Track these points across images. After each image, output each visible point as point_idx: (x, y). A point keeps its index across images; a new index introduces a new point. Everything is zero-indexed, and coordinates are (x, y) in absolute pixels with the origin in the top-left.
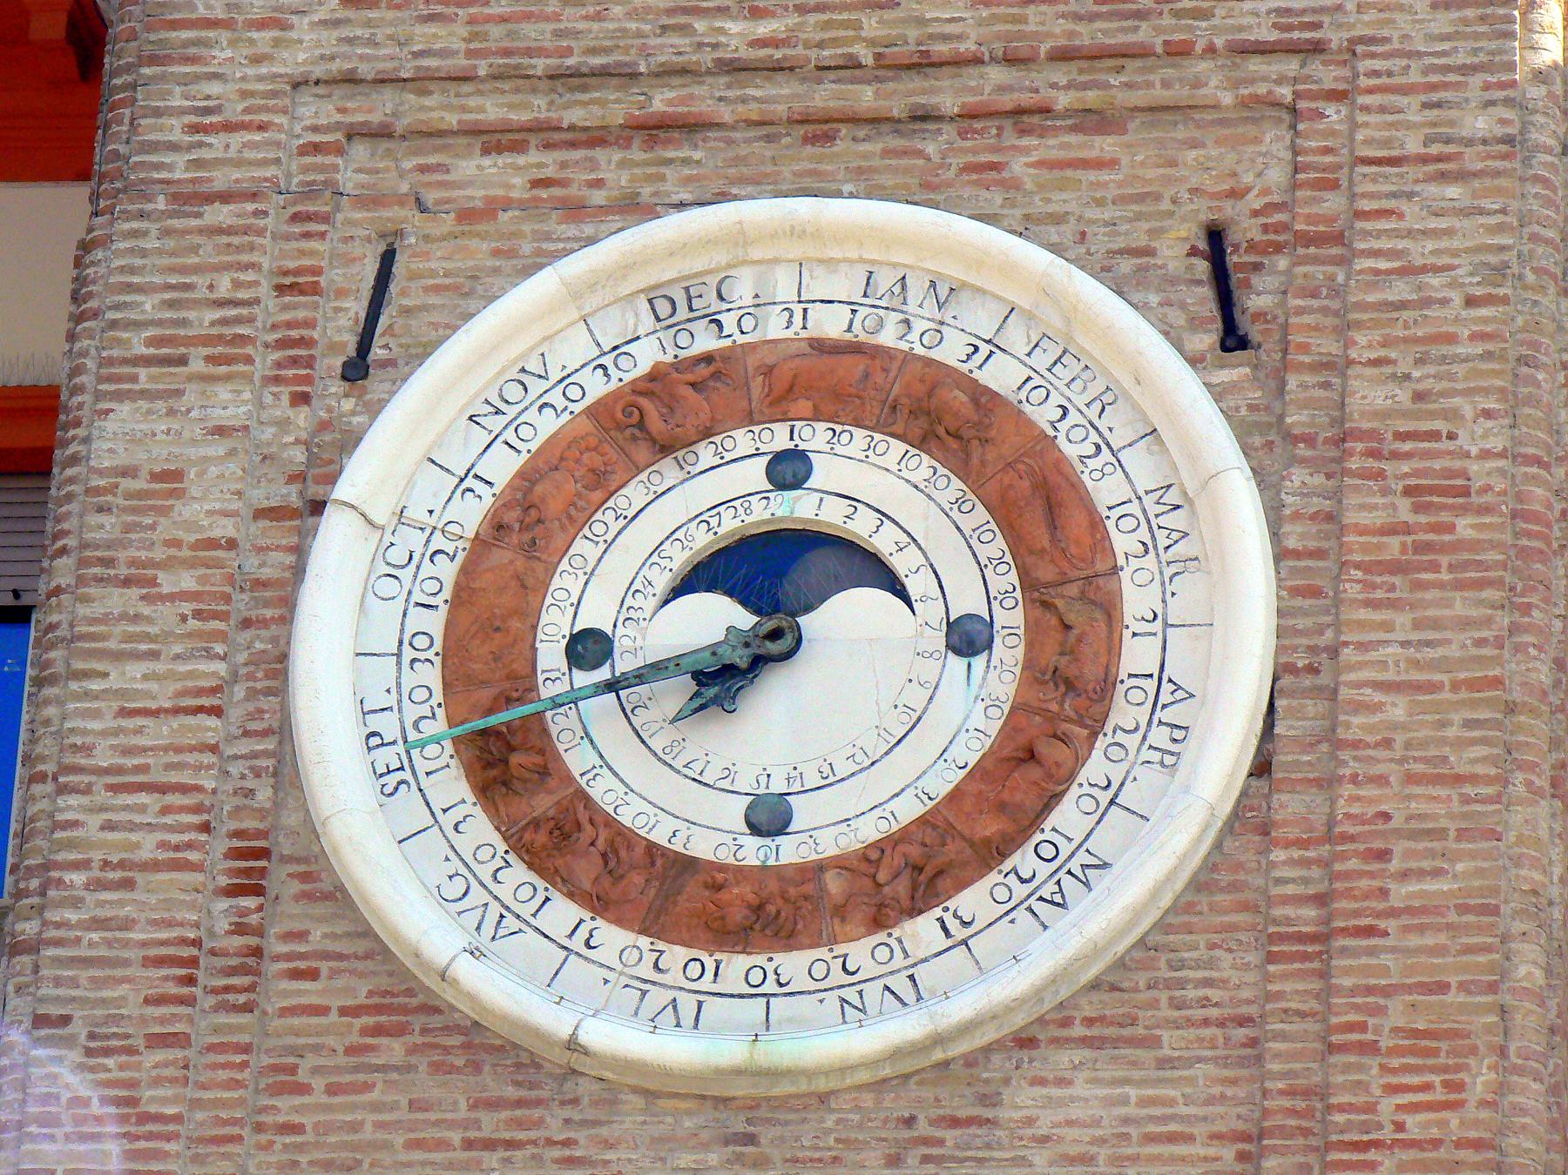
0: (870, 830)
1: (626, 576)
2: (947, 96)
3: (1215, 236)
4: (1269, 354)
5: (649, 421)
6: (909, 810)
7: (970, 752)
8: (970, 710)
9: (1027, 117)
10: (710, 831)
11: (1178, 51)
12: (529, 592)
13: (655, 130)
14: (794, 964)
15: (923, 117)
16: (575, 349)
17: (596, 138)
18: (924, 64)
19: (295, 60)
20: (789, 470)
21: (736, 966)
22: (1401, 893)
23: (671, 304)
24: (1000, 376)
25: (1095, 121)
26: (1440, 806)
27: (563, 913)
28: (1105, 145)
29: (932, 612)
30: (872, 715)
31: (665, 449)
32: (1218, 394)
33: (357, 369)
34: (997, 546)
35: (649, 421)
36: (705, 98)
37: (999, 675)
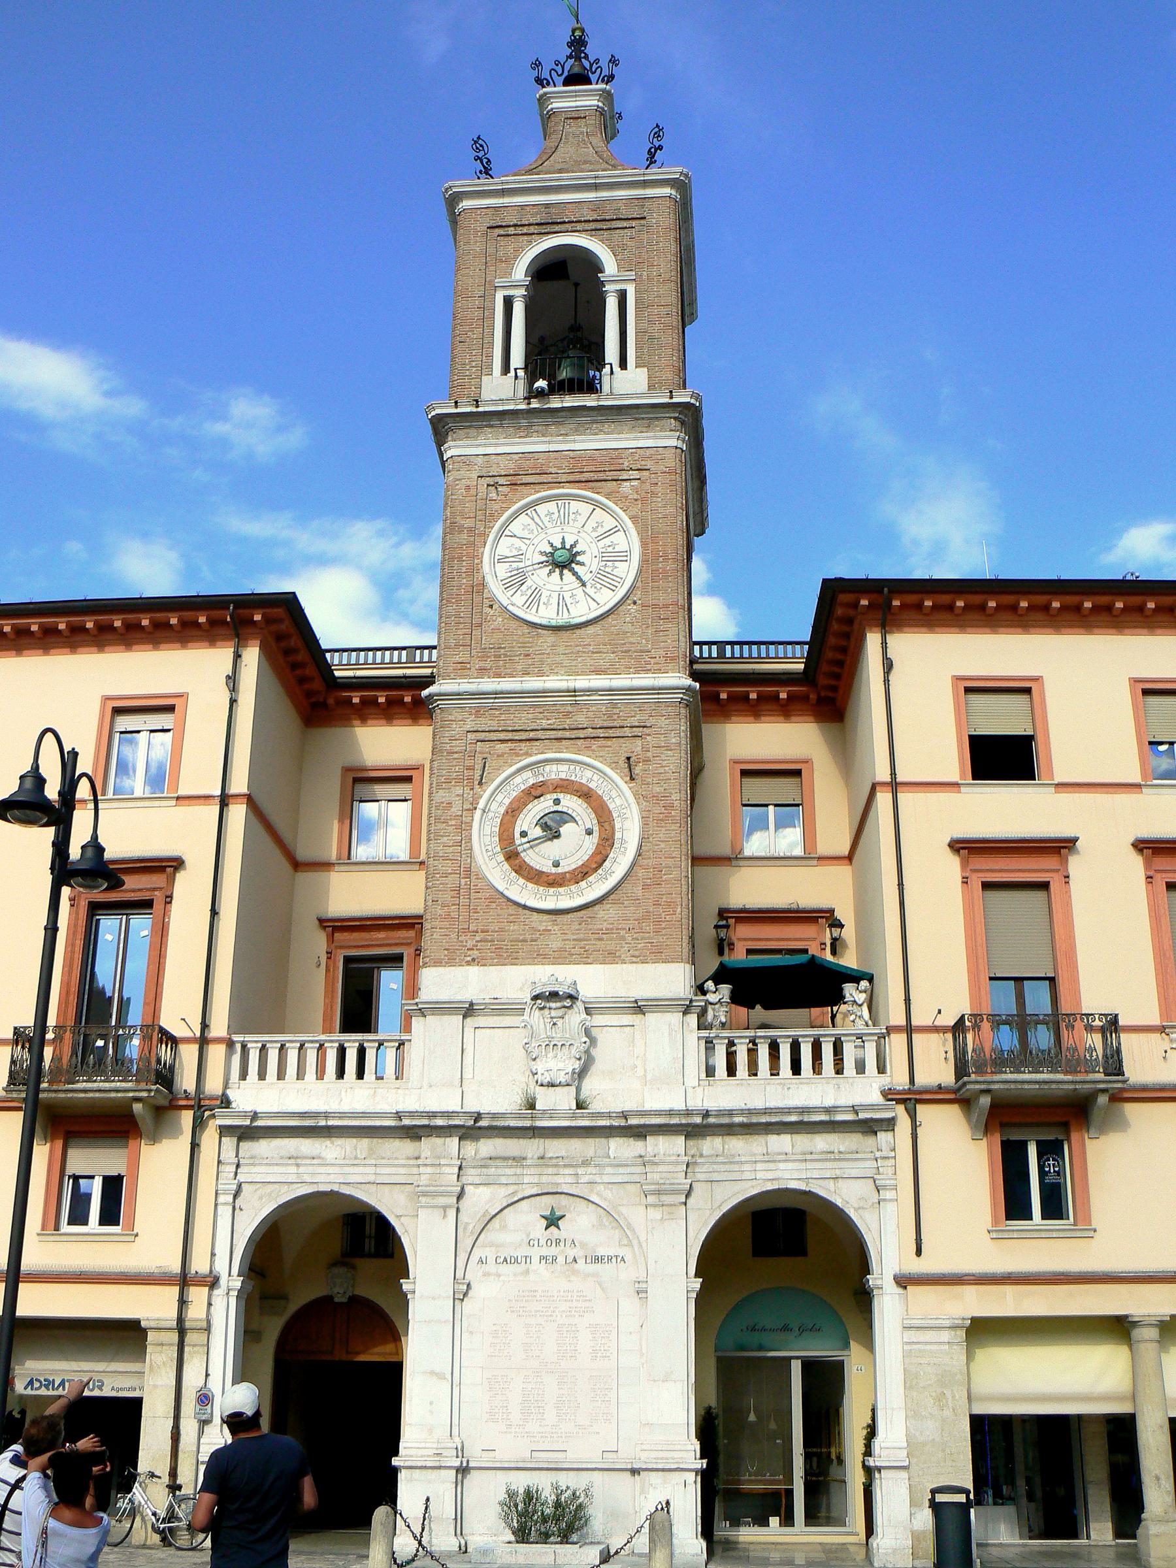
1: (528, 821)
2: (581, 734)
4: (639, 781)
6: (580, 863)
7: (590, 852)
8: (590, 845)
10: (547, 867)
14: (561, 890)
19: (468, 727)
20: (557, 802)
21: (552, 890)
24: (592, 785)
26: (670, 862)
27: (522, 881)
28: (609, 743)
30: (573, 845)
33: (480, 783)
35: (534, 793)
36: (540, 734)
37: (595, 838)
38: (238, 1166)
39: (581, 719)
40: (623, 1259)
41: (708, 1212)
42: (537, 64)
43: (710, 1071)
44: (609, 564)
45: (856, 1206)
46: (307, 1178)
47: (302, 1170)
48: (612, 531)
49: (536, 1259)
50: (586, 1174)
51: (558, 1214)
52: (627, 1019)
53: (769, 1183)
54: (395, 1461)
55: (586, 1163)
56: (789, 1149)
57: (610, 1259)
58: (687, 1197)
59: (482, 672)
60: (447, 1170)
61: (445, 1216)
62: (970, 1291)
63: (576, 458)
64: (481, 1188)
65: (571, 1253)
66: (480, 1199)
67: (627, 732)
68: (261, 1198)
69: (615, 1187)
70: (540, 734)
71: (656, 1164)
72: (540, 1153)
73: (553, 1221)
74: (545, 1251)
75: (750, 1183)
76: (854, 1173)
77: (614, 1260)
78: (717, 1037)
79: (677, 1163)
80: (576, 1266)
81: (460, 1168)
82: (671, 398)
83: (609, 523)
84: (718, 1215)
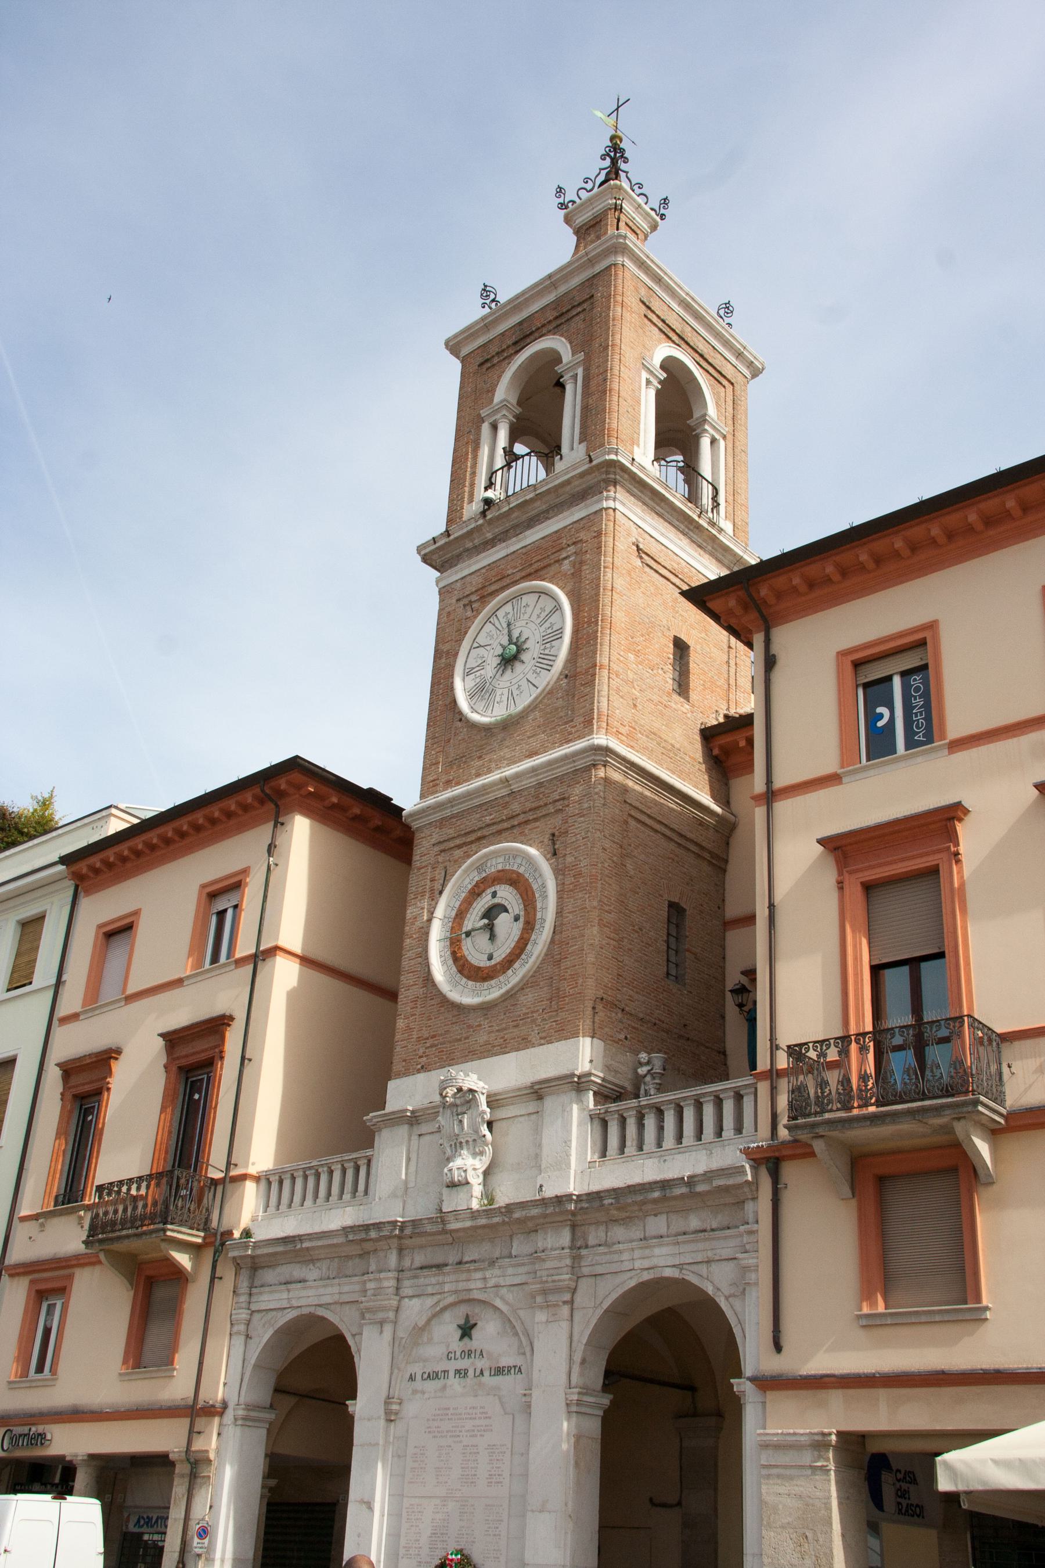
0: (503, 956)
3: (553, 835)
5: (475, 893)
6: (508, 951)
7: (516, 939)
8: (517, 929)
9: (527, 822)
11: (546, 805)
12: (461, 925)
13: (479, 839)
14: (493, 982)
15: (513, 827)
16: (467, 880)
17: (472, 842)
18: (513, 817)
19: (433, 841)
22: (571, 950)
23: (479, 869)
24: (521, 870)
25: (536, 820)
29: (512, 915)
31: (479, 895)
32: (551, 865)
34: (520, 901)
35: (475, 893)
36: (485, 832)
37: (520, 924)
38: (250, 1294)
39: (515, 807)
40: (520, 1370)
41: (591, 1310)
42: (560, 190)
43: (604, 1154)
44: (548, 645)
45: (727, 1293)
46: (295, 1303)
47: (291, 1295)
48: (552, 612)
49: (452, 1374)
50: (493, 1276)
51: (472, 1322)
52: (532, 1107)
53: (645, 1272)
55: (492, 1263)
56: (663, 1231)
57: (509, 1369)
58: (573, 1293)
59: (448, 784)
60: (386, 1284)
61: (381, 1332)
62: (836, 1398)
64: (415, 1300)
65: (480, 1364)
66: (415, 1310)
68: (264, 1326)
69: (516, 1288)
70: (485, 832)
71: (544, 1260)
72: (457, 1259)
73: (467, 1330)
74: (462, 1364)
75: (629, 1274)
76: (726, 1253)
77: (512, 1371)
78: (606, 1112)
79: (560, 1258)
81: (398, 1280)
82: (591, 461)
83: (548, 604)
84: (599, 1312)
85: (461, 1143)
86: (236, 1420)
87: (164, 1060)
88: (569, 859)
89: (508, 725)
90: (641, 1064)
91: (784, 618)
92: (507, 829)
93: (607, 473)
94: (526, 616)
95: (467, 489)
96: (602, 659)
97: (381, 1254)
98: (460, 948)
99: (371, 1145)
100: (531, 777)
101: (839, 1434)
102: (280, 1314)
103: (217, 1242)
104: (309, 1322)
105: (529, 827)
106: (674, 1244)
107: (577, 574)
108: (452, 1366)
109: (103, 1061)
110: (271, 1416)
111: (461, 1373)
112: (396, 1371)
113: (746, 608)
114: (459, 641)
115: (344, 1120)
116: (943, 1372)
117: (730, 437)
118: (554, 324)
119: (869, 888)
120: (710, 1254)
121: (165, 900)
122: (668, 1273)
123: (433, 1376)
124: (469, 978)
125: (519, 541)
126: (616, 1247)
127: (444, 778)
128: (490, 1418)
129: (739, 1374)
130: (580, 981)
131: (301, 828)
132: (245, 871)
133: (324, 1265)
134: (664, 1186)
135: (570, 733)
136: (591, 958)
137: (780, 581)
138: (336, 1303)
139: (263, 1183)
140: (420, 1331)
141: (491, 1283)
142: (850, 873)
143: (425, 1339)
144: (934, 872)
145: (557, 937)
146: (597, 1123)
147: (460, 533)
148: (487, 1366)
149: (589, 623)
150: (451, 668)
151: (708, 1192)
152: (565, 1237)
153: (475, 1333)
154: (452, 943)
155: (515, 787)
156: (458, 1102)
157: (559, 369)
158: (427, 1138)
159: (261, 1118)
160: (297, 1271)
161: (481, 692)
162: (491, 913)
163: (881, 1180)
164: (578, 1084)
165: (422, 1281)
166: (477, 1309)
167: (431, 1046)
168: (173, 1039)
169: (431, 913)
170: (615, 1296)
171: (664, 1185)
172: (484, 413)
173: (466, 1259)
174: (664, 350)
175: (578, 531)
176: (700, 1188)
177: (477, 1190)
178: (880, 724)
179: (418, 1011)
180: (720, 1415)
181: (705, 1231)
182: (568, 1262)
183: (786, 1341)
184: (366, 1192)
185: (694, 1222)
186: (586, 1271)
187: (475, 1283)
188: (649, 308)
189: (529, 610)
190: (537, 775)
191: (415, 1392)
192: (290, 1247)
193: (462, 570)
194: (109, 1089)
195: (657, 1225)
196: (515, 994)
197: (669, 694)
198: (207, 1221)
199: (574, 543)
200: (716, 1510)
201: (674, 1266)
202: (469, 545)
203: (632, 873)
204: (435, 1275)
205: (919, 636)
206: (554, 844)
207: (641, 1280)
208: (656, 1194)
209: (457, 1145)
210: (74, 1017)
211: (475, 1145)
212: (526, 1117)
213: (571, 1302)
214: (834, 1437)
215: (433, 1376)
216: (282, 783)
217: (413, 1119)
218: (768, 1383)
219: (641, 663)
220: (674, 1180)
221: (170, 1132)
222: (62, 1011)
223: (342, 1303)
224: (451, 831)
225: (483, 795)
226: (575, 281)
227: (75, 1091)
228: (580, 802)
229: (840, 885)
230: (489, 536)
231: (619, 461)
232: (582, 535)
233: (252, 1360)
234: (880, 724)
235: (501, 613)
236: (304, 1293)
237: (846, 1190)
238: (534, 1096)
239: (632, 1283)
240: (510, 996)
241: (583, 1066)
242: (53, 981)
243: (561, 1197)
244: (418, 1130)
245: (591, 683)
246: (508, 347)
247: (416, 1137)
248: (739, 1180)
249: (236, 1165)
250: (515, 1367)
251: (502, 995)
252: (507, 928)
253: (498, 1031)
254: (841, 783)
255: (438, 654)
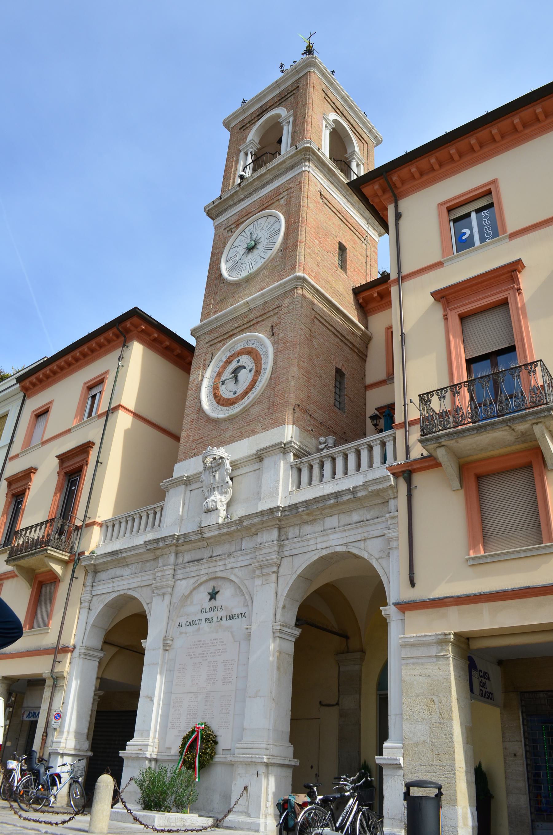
2: (251, 323)
3: (272, 326)
8: (250, 376)
9: (257, 323)
11: (269, 312)
15: (250, 326)
16: (224, 357)
18: (250, 321)
19: (206, 341)
22: (281, 380)
24: (254, 347)
25: (263, 320)
28: (264, 322)
29: (248, 370)
31: (230, 363)
35: (228, 362)
36: (235, 332)
37: (253, 373)
38: (92, 586)
39: (252, 316)
42: (282, 65)
43: (299, 487)
45: (377, 557)
46: (116, 589)
48: (274, 223)
49: (203, 621)
51: (217, 590)
52: (256, 466)
53: (324, 550)
54: (122, 753)
55: (230, 555)
56: (336, 524)
61: (163, 600)
62: (453, 612)
63: (261, 199)
64: (184, 581)
65: (220, 614)
66: (183, 586)
67: (272, 313)
70: (235, 332)
71: (261, 549)
72: (209, 556)
73: (213, 595)
74: (209, 615)
76: (376, 533)
78: (301, 463)
79: (271, 547)
80: (222, 622)
81: (174, 570)
82: (297, 148)
83: (272, 220)
84: (295, 577)
85: (214, 488)
86: (80, 655)
87: (58, 469)
88: (281, 335)
89: (248, 280)
90: (321, 443)
91: (406, 194)
92: (247, 328)
93: (305, 154)
94: (260, 228)
95: (231, 181)
96: (301, 238)
97: (166, 556)
98: (218, 391)
99: (164, 499)
100: (261, 299)
101: (456, 634)
102: (108, 595)
103: (76, 559)
104: (126, 600)
105: (259, 325)
106: (343, 531)
107: (288, 203)
108: (204, 617)
109: (27, 475)
110: (101, 655)
111: (209, 620)
112: (170, 622)
113: (384, 191)
114: (224, 247)
115: (150, 490)
116: (529, 588)
117: (366, 165)
118: (278, 103)
119: (463, 318)
120: (366, 534)
121: (65, 395)
122: (339, 549)
123: (192, 623)
124: (222, 405)
125: (257, 195)
126: (306, 537)
127: (214, 310)
128: (225, 644)
129: (385, 604)
130: (286, 395)
131: (137, 351)
132: (107, 372)
133: (133, 568)
134: (337, 496)
135: (282, 276)
136: (293, 383)
137: (404, 172)
138: (139, 587)
139: (104, 527)
140: (186, 597)
141: (229, 567)
142: (451, 310)
143: (189, 603)
144: (504, 303)
145: (273, 376)
146: (295, 472)
147: (227, 196)
148: (225, 615)
149: (294, 223)
150: (219, 259)
151: (365, 497)
152: (274, 534)
153: (218, 596)
154: (214, 389)
155: (252, 306)
156: (213, 465)
157: (280, 120)
158: (196, 491)
159: (106, 493)
160: (118, 571)
161: (235, 267)
162: (235, 372)
163: (479, 478)
164: (283, 448)
165: (188, 570)
166: (220, 583)
167: (200, 443)
168: (63, 458)
169: (203, 376)
170: (304, 566)
171: (337, 495)
172: (241, 148)
173: (214, 555)
174: (333, 116)
175: (289, 184)
176: (360, 494)
177: (222, 512)
178: (464, 238)
179: (193, 427)
180: (363, 651)
181: (363, 521)
182: (276, 548)
183: (417, 580)
184: (159, 525)
185: (355, 517)
186: (286, 553)
187: (219, 568)
188: (327, 95)
189: (262, 225)
190: (264, 298)
191: (181, 633)
192: (115, 557)
193: (227, 215)
194: (29, 488)
195: (332, 522)
196: (248, 409)
197: (336, 267)
198: (72, 548)
199: (287, 190)
200: (360, 706)
201: (342, 544)
202: (231, 203)
203: (316, 347)
204: (196, 566)
205: (488, 188)
206: (272, 330)
207: (321, 555)
208: (332, 501)
209: (212, 489)
210: (17, 456)
211: (222, 488)
212: (253, 473)
213: (277, 572)
214: (452, 636)
215: (192, 623)
216: (128, 324)
217: (188, 482)
218: (404, 607)
219: (322, 247)
220: (343, 491)
221: (58, 506)
222: (11, 454)
223: (142, 587)
224: (216, 334)
225: (234, 313)
226: (289, 83)
227: (13, 492)
228: (288, 307)
229: (446, 318)
230: (242, 197)
231: (311, 148)
232: (291, 185)
233: (91, 621)
234: (464, 238)
235: (246, 230)
236: (122, 583)
237: (457, 484)
238: (258, 460)
239: (316, 558)
240: (246, 410)
241: (287, 438)
242: (9, 442)
243: (273, 508)
244: (190, 488)
245: (295, 250)
246: (255, 118)
247: (189, 492)
248: (386, 485)
249: (90, 518)
250: (241, 614)
251: (241, 410)
252: (245, 377)
253: (238, 429)
254: (443, 266)
255: (213, 255)
